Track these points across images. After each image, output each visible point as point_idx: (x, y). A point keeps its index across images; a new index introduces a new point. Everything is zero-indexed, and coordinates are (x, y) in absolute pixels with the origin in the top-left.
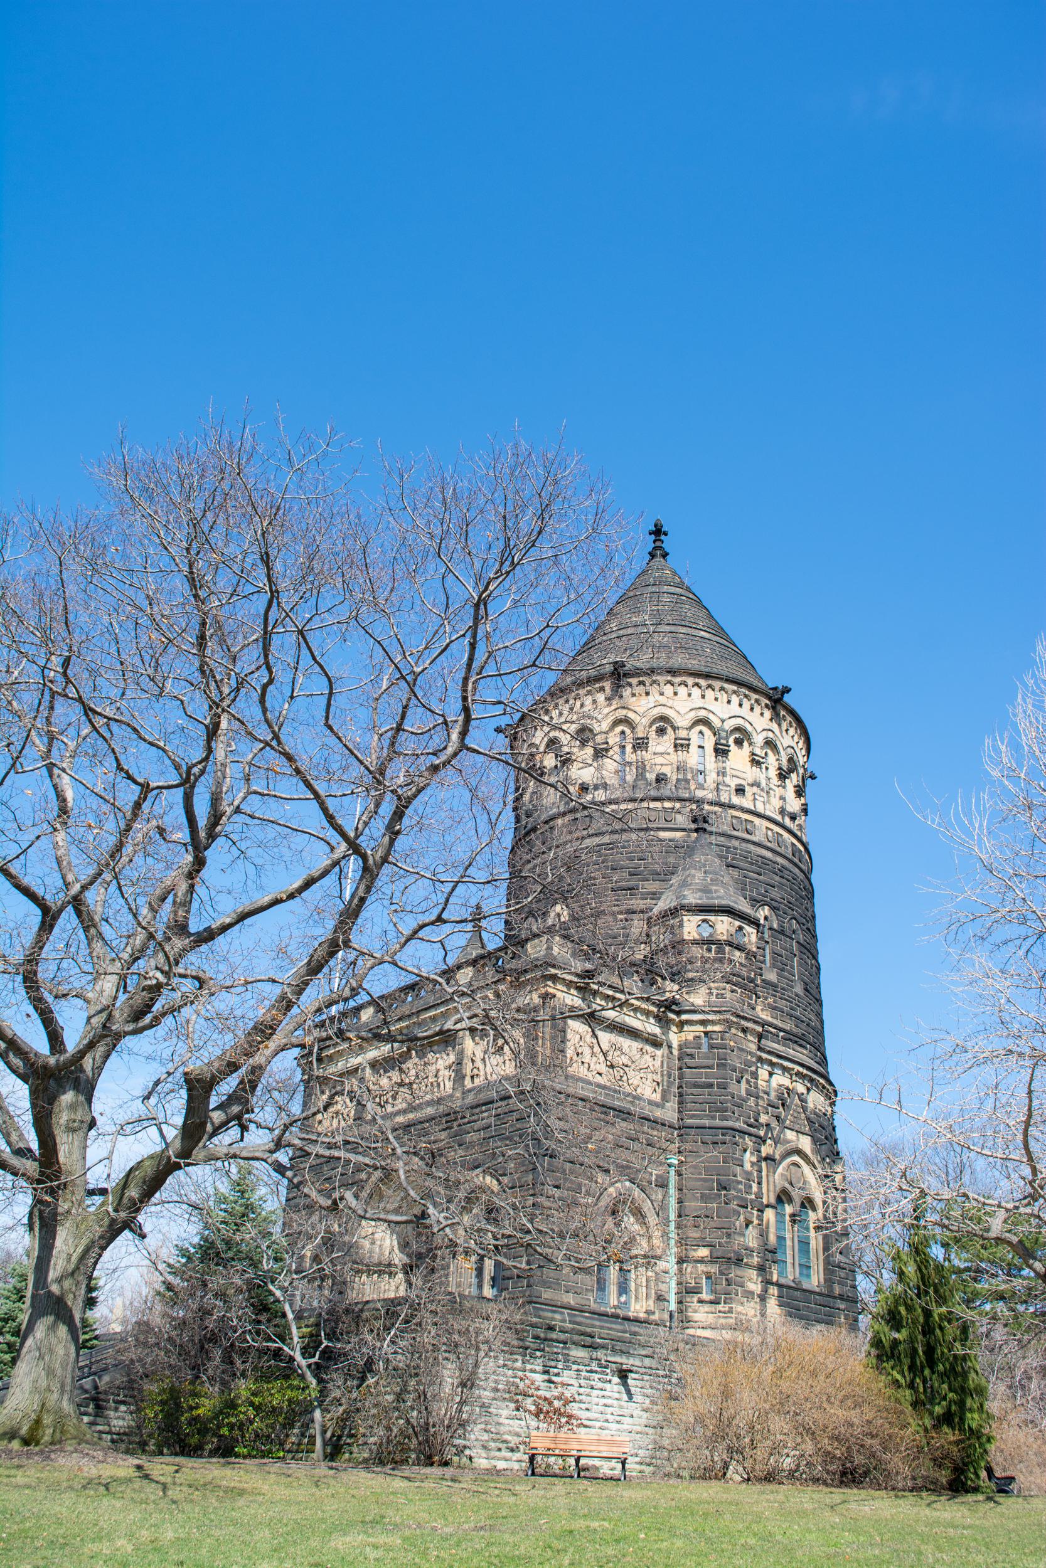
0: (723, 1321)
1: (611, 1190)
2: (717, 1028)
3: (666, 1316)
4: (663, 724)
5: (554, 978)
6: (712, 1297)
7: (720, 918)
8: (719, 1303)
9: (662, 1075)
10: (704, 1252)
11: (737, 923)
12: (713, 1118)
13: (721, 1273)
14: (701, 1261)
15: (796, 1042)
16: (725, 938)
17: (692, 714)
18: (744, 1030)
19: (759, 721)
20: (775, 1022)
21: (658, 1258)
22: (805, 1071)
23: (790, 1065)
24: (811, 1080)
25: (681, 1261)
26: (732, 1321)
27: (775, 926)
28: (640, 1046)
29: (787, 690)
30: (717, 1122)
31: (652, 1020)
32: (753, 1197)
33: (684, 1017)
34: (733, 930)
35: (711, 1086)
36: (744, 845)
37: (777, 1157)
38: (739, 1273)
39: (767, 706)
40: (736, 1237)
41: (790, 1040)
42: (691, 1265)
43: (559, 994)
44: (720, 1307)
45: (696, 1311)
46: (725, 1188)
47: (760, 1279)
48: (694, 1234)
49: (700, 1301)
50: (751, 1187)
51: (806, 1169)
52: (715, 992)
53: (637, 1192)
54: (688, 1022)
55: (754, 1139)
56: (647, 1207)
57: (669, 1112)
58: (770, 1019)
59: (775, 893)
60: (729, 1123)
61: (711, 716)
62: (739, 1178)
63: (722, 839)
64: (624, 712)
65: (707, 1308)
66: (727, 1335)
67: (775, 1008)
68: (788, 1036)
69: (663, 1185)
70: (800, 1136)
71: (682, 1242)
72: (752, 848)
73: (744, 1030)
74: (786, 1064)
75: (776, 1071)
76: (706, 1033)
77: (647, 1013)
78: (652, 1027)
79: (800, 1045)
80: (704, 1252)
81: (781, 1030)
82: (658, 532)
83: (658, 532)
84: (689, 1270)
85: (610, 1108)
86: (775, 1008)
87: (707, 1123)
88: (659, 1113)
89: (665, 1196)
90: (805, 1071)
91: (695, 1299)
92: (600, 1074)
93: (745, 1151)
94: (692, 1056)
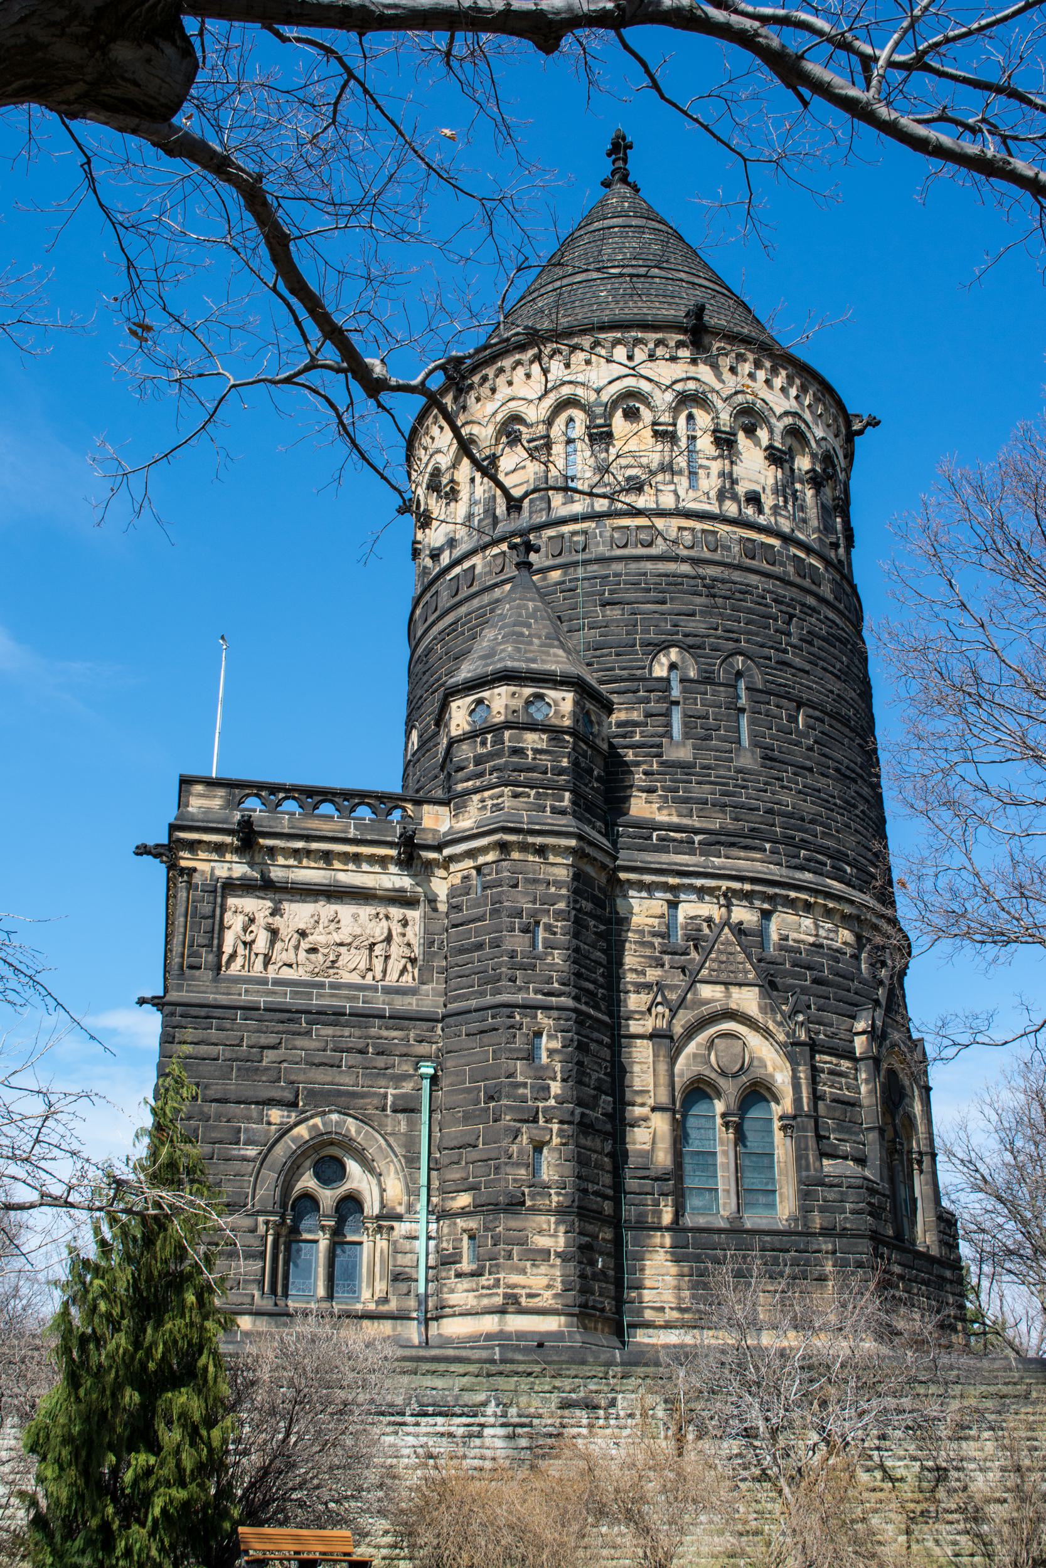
0: (485, 1302)
1: (302, 1131)
2: (491, 857)
3: (412, 1303)
4: (510, 429)
5: (192, 846)
6: (474, 1267)
7: (496, 691)
8: (481, 1275)
10: (464, 1200)
11: (528, 691)
12: (483, 994)
13: (486, 1229)
14: (463, 1213)
15: (733, 845)
18: (541, 851)
19: (667, 372)
20: (686, 821)
21: (399, 1218)
22: (747, 887)
23: (712, 883)
24: (770, 898)
26: (498, 1300)
27: (692, 674)
28: (374, 912)
30: (489, 1000)
31: (393, 869)
32: (552, 1102)
33: (446, 852)
34: (518, 703)
35: (480, 946)
36: (633, 566)
37: (678, 1030)
38: (513, 1223)
39: (680, 344)
40: (509, 1170)
41: (718, 843)
43: (200, 866)
44: (484, 1281)
45: (452, 1291)
47: (562, 1229)
48: (455, 1174)
49: (459, 1275)
50: (548, 1088)
51: (754, 1040)
52: (489, 803)
53: (352, 1125)
54: (451, 859)
55: (555, 1014)
58: (675, 819)
59: (697, 625)
60: (504, 998)
61: (580, 391)
62: (520, 1079)
63: (595, 567)
65: (466, 1284)
66: (490, 1324)
67: (686, 801)
68: (714, 838)
70: (734, 990)
72: (649, 566)
73: (541, 851)
74: (699, 882)
75: (683, 897)
76: (478, 869)
77: (383, 861)
78: (395, 879)
79: (746, 848)
80: (464, 1200)
81: (697, 832)
82: (619, 148)
83: (619, 148)
85: (297, 1012)
86: (686, 801)
87: (473, 1003)
88: (409, 1004)
89: (413, 1126)
90: (747, 887)
91: (452, 1273)
92: (290, 966)
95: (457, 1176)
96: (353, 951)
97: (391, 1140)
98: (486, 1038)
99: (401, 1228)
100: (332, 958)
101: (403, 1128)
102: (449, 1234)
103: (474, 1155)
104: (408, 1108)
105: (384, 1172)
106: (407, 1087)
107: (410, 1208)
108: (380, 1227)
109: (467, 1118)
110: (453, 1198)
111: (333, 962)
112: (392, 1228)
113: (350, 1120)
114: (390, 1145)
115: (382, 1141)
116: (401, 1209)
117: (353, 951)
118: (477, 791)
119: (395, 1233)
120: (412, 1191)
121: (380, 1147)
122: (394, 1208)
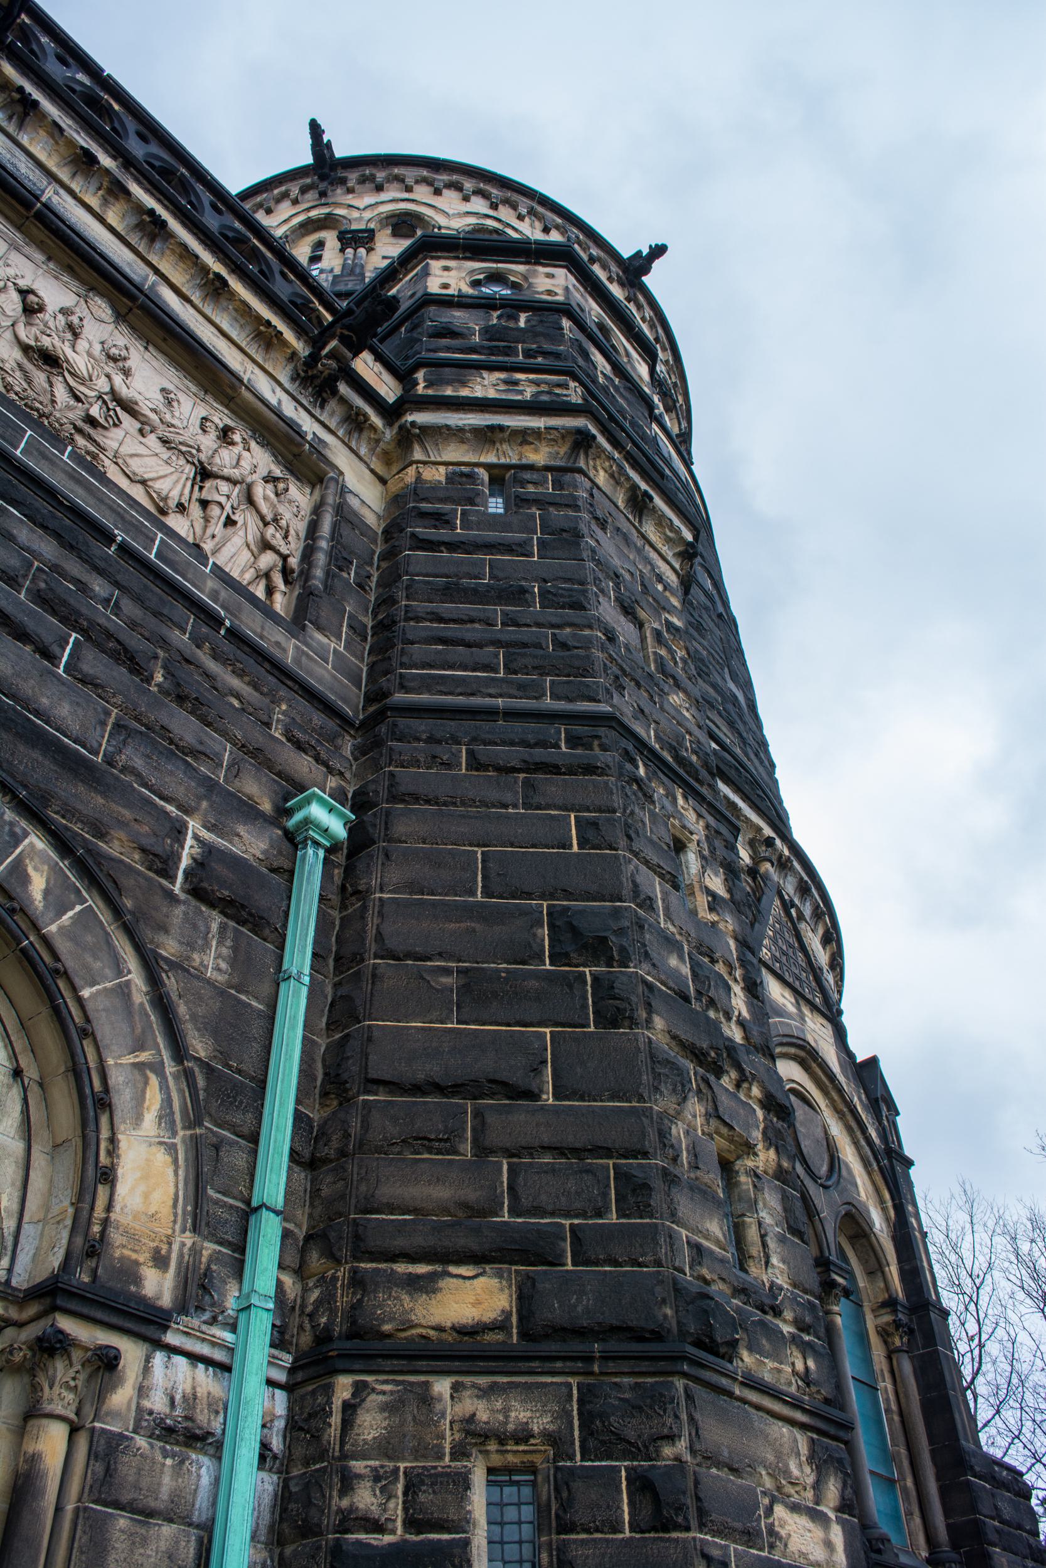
2: (538, 456)
9: (308, 554)
10: (472, 1298)
16: (560, 298)
17: (472, 220)
21: (148, 1324)
25: (316, 1356)
29: (659, 251)
42: (383, 1387)
46: (598, 948)
56: (109, 984)
57: (327, 657)
64: (326, 210)
69: (245, 904)
71: (332, 1233)
80: (472, 1298)
84: (371, 1424)
89: (262, 970)
93: (679, 846)
94: (441, 519)
95: (442, 1193)
96: (152, 440)
97: (171, 983)
98: (553, 787)
99: (158, 1379)
100: (95, 411)
101: (213, 962)
102: (386, 1448)
103: (514, 1123)
104: (245, 904)
105: (122, 1099)
106: (252, 844)
107: (198, 1291)
108: (53, 1346)
109: (476, 993)
110: (423, 1286)
111: (91, 421)
112: (106, 1363)
113: (36, 841)
114: (162, 1003)
115: (136, 977)
116: (159, 1286)
117: (152, 440)
118: (492, 368)
119: (121, 1397)
120: (218, 1210)
121: (124, 991)
122: (130, 1273)
